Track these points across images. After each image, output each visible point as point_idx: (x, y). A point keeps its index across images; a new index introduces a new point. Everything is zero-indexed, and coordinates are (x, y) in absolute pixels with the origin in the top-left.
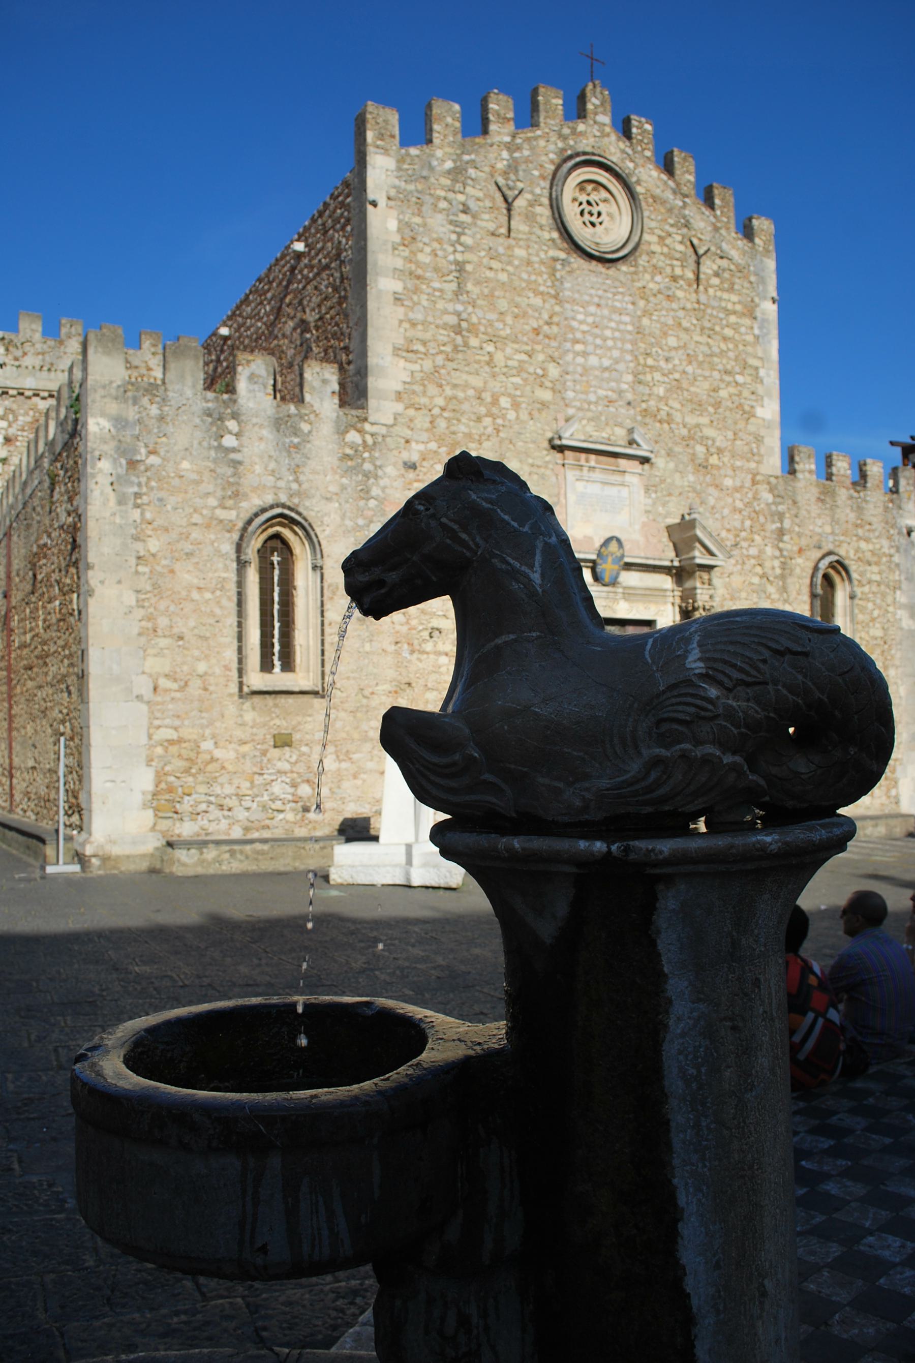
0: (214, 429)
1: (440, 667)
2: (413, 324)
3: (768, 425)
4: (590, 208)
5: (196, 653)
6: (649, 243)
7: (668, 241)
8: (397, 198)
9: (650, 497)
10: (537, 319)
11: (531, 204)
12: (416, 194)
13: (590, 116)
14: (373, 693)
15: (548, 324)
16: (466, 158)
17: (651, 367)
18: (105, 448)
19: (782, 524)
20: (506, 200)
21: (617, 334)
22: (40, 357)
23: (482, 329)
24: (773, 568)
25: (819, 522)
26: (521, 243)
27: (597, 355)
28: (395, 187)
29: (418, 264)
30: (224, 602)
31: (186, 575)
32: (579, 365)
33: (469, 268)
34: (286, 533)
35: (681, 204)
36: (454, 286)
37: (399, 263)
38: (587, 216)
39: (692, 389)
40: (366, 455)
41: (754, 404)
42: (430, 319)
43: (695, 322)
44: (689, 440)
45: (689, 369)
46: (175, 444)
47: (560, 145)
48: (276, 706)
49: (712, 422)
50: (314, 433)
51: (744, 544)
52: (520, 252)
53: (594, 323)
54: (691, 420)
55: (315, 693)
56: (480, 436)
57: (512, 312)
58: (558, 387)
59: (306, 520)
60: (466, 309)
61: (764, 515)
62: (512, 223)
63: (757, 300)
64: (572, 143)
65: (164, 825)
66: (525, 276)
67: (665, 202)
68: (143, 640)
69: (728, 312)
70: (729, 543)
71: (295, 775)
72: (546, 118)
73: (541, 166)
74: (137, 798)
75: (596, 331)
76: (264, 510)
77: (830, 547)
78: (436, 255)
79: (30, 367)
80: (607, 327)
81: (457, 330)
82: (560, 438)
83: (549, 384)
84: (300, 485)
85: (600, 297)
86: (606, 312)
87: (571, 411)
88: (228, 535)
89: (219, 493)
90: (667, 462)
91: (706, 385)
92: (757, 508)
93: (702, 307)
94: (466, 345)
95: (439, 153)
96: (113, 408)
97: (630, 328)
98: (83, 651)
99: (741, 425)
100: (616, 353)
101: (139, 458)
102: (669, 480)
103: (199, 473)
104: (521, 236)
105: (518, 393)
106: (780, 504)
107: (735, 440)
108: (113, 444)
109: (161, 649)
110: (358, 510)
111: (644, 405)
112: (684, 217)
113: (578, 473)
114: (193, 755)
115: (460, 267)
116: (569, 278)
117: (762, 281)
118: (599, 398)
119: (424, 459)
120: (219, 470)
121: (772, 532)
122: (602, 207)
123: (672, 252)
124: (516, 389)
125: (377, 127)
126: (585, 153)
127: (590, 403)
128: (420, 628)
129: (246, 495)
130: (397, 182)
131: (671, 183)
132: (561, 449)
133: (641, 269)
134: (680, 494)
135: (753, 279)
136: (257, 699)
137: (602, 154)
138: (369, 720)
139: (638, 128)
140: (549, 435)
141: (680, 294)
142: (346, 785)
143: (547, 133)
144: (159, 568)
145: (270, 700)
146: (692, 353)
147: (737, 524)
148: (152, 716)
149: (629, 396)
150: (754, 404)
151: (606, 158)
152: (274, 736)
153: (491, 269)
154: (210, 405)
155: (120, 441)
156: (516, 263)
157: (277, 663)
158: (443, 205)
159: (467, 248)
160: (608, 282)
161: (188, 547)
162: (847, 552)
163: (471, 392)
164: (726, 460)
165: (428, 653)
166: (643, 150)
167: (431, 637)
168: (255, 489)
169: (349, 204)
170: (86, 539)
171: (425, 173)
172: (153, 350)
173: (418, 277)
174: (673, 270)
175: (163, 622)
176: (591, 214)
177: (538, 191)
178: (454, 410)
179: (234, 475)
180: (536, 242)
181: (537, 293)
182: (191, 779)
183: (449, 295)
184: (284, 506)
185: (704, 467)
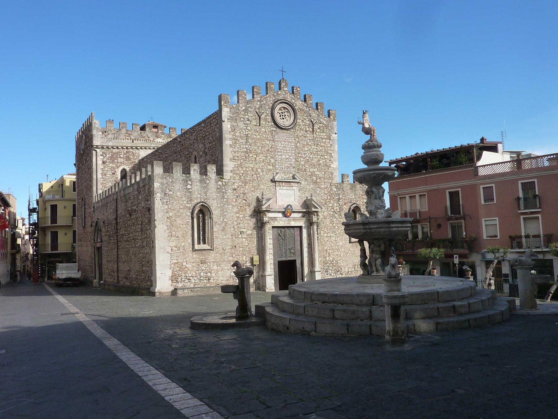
0: (185, 184)
1: (243, 241)
2: (235, 152)
3: (335, 169)
4: (282, 114)
5: (182, 241)
6: (299, 122)
7: (305, 121)
8: (230, 119)
9: (300, 192)
10: (268, 147)
11: (266, 116)
12: (235, 117)
13: (282, 88)
14: (226, 249)
15: (270, 148)
16: (248, 105)
17: (300, 157)
18: (159, 190)
19: (339, 197)
20: (259, 116)
21: (290, 149)
22: (113, 135)
23: (253, 151)
24: (337, 209)
25: (351, 195)
26: (263, 127)
27: (284, 155)
28: (229, 116)
29: (236, 136)
30: (188, 227)
31: (179, 221)
32: (280, 158)
33: (249, 135)
34: (204, 209)
35: (308, 110)
36: (245, 141)
37: (231, 136)
38: (281, 116)
39: (312, 161)
40: (223, 187)
41: (330, 163)
42: (239, 150)
43: (312, 143)
44: (311, 176)
45: (311, 156)
46: (176, 188)
47: (274, 98)
48: (201, 253)
49: (318, 170)
50: (210, 183)
51: (328, 203)
52: (263, 130)
53: (284, 146)
54: (312, 170)
55: (211, 250)
56: (253, 180)
57: (261, 146)
58: (274, 164)
59: (208, 205)
60: (249, 147)
61: (334, 195)
62: (261, 122)
63: (331, 134)
64: (277, 97)
65: (174, 284)
66: (264, 136)
67: (303, 110)
68: (169, 238)
69: (322, 139)
70: (323, 203)
71: (207, 271)
72: (270, 91)
73: (269, 105)
74: (168, 278)
75: (284, 148)
76: (198, 204)
77: (355, 202)
78: (241, 133)
79: (110, 138)
80: (287, 147)
81: (246, 152)
82: (274, 179)
83: (272, 164)
84: (207, 197)
85: (285, 139)
86: (287, 143)
87: (278, 171)
88: (189, 210)
89: (187, 200)
90: (305, 182)
91: (316, 160)
92: (332, 193)
93: (315, 138)
94: (249, 156)
95: (241, 105)
96: (160, 180)
97: (294, 147)
98: (153, 241)
99: (327, 170)
100: (290, 154)
101: (167, 192)
102: (305, 187)
103: (181, 195)
104: (263, 125)
105: (263, 167)
106: (339, 191)
107: (325, 174)
108: (160, 189)
109: (173, 240)
110: (221, 202)
111: (298, 167)
112: (309, 113)
113: (279, 187)
114: (181, 266)
115: (247, 135)
116: (276, 135)
117: (332, 128)
118: (285, 167)
119: (238, 187)
120: (186, 194)
121: (336, 199)
122: (286, 114)
123: (306, 124)
124: (262, 167)
125: (224, 100)
126: (281, 100)
127: (283, 168)
128: (238, 231)
129: (193, 201)
130: (230, 115)
131: (305, 104)
132: (275, 182)
133: (297, 130)
134: (309, 191)
135: (330, 128)
136: (197, 252)
137: (286, 99)
138: (225, 256)
139: (296, 90)
140: (272, 178)
141: (308, 135)
142: (219, 273)
143: (270, 96)
144: (173, 220)
145: (200, 252)
146: (312, 151)
147: (326, 198)
148: (171, 257)
149: (294, 165)
150: (330, 163)
151: (287, 101)
152: (201, 261)
153: (255, 135)
154: (184, 178)
155: (162, 188)
156: (262, 133)
157: (201, 242)
158: (242, 119)
159: (249, 130)
160: (287, 135)
161: (179, 214)
162: (360, 203)
163: (250, 169)
164: (322, 180)
165: (240, 238)
166: (297, 96)
167: (241, 234)
168: (195, 198)
169: (217, 119)
170: (154, 213)
171: (237, 111)
172: (150, 131)
173: (236, 140)
174: (306, 129)
175: (174, 233)
176: (283, 116)
177: (268, 112)
178: (246, 174)
179: (190, 195)
180: (267, 126)
181: (267, 140)
182: (181, 272)
183: (244, 143)
184: (203, 202)
185: (315, 183)
